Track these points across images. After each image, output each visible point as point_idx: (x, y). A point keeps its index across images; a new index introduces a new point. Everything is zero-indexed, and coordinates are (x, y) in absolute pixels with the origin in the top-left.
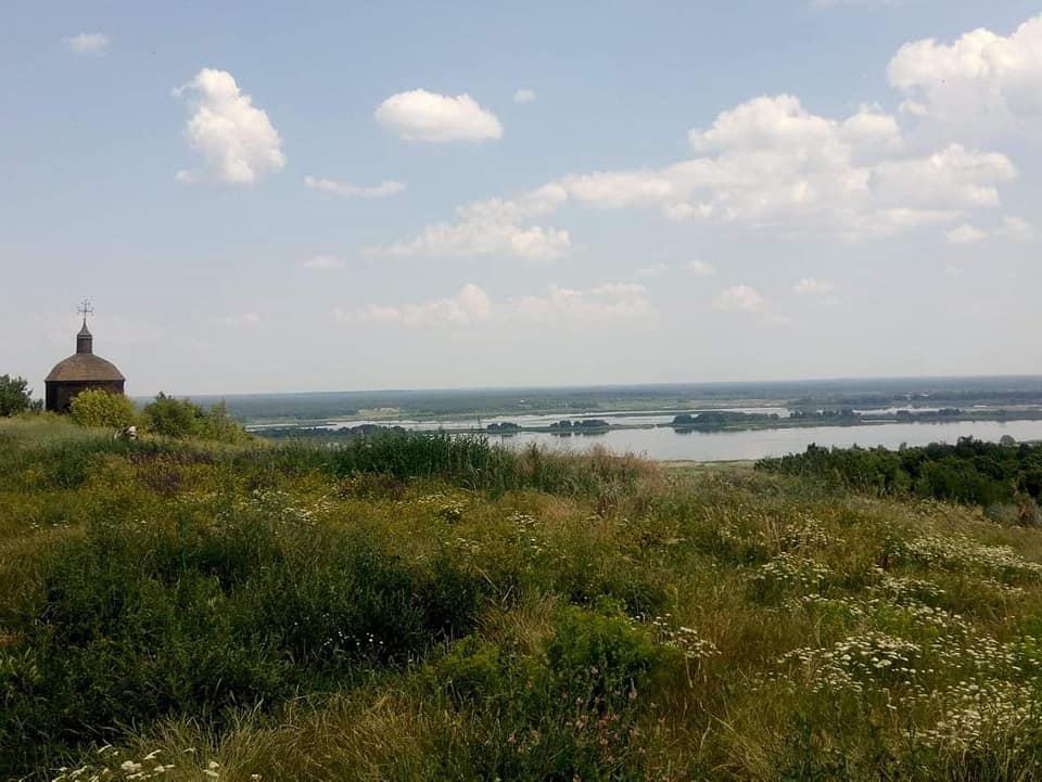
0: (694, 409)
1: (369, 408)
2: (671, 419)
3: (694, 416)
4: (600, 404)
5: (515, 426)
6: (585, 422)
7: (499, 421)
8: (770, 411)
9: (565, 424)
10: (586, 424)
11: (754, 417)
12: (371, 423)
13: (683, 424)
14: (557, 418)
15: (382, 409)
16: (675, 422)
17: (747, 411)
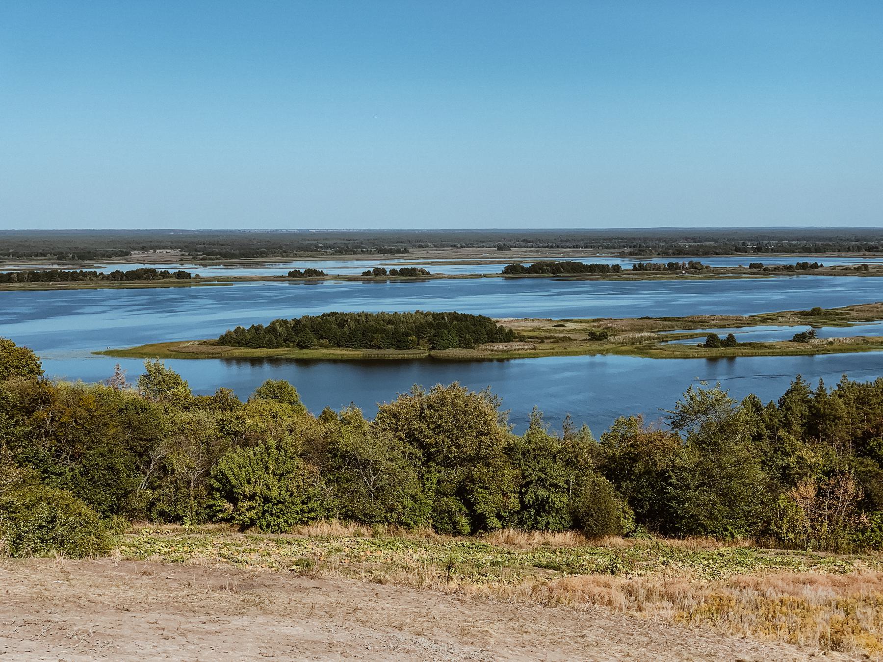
0: (527, 258)
1: (144, 249)
2: (501, 268)
4: (410, 250)
5: (321, 273)
6: (402, 270)
7: (301, 266)
8: (611, 262)
9: (378, 272)
10: (403, 272)
11: (592, 268)
12: (148, 266)
13: (513, 271)
14: (370, 265)
15: (158, 251)
16: (504, 272)
17: (587, 262)
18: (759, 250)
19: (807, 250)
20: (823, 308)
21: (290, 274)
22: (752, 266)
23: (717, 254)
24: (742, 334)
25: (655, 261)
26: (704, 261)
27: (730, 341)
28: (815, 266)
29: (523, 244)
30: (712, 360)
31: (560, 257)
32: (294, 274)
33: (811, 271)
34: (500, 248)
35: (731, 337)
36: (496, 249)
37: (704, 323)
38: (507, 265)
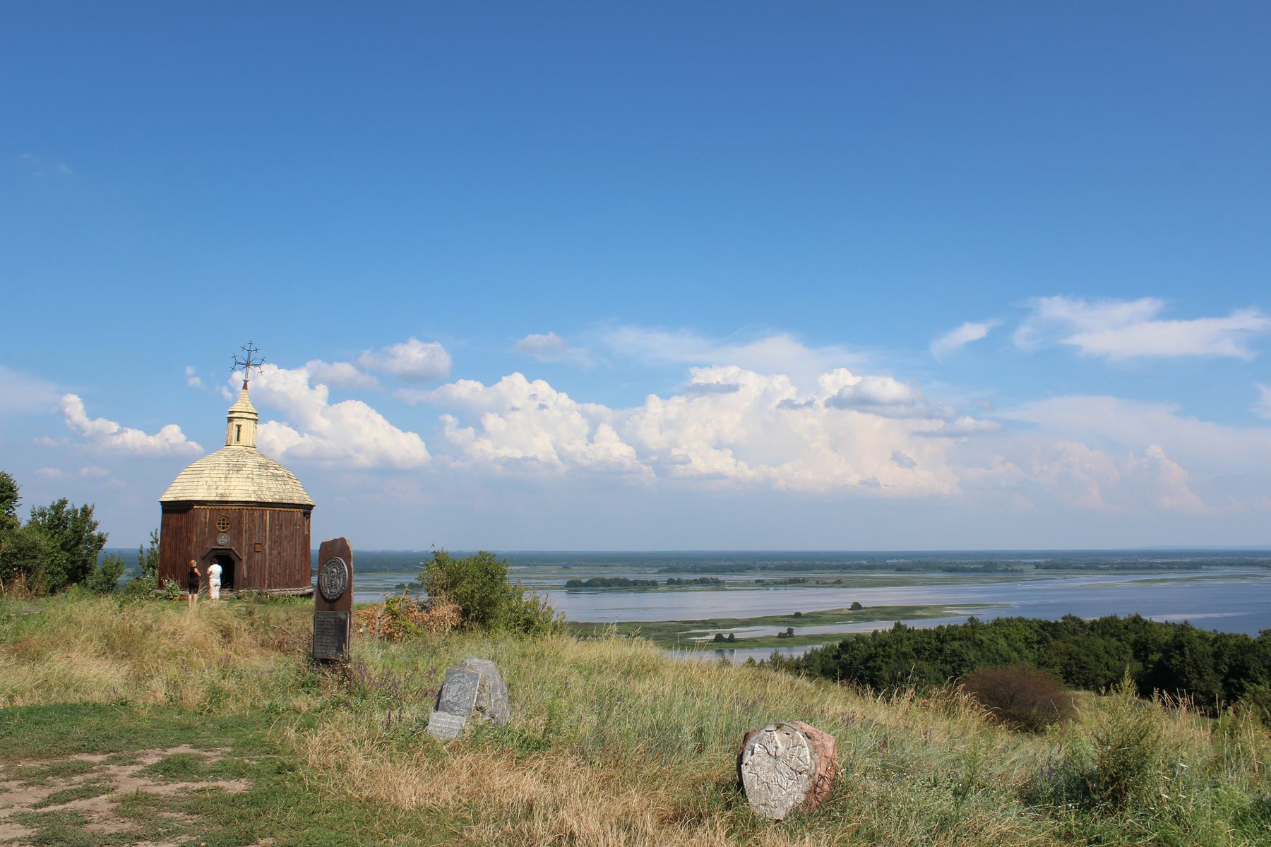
0: (584, 577)
2: (564, 582)
3: (584, 581)
13: (574, 587)
16: (566, 586)
18: (764, 568)
19: (799, 569)
20: (804, 612)
21: (397, 587)
22: (757, 581)
23: (733, 571)
24: (741, 633)
25: (685, 577)
26: (721, 577)
27: (731, 639)
28: (804, 581)
29: (584, 563)
30: (720, 651)
31: (608, 575)
32: (401, 587)
33: (802, 584)
34: (565, 567)
35: (732, 636)
36: (561, 567)
37: (714, 624)
38: (568, 580)
